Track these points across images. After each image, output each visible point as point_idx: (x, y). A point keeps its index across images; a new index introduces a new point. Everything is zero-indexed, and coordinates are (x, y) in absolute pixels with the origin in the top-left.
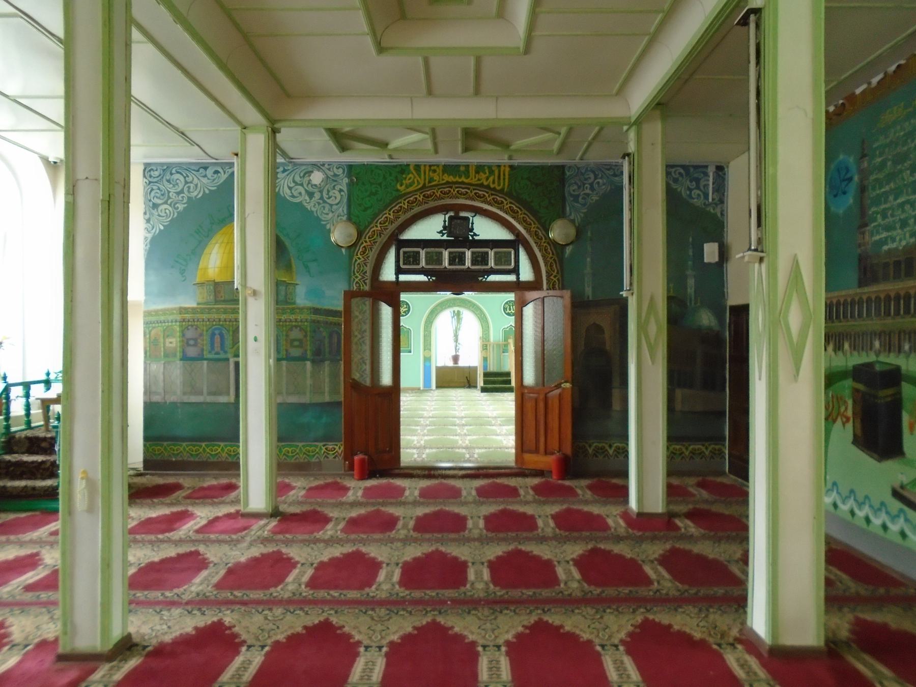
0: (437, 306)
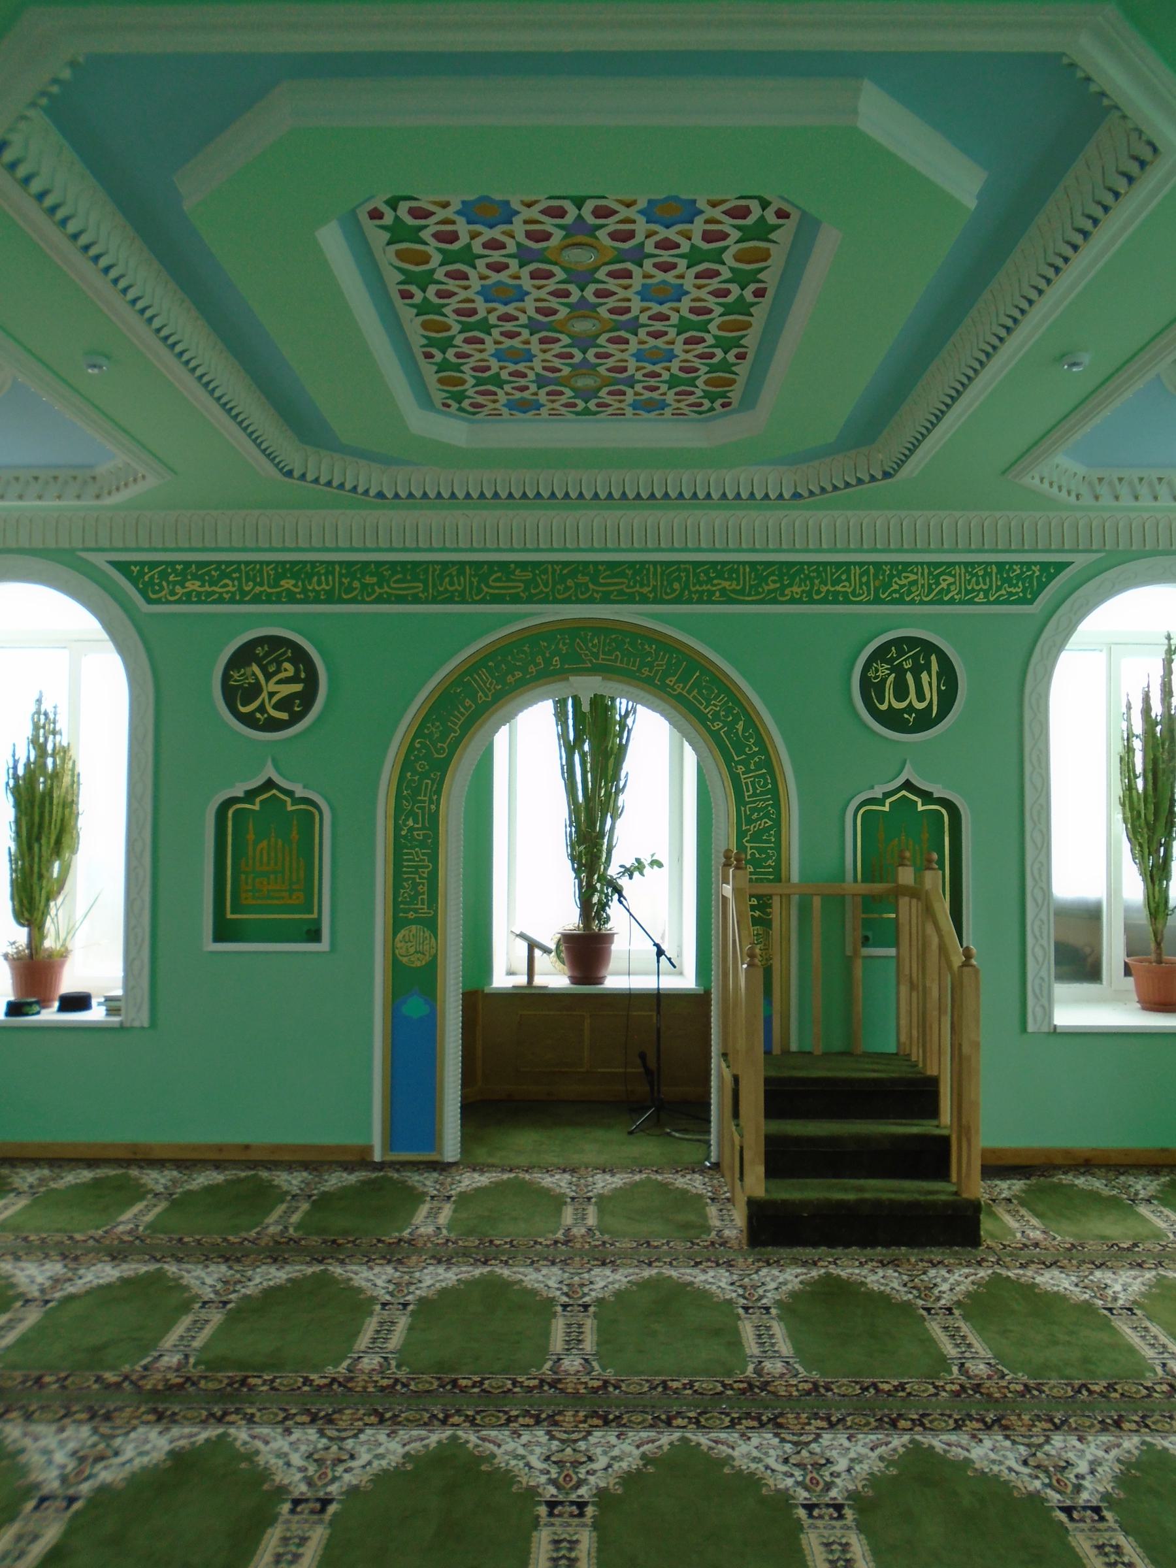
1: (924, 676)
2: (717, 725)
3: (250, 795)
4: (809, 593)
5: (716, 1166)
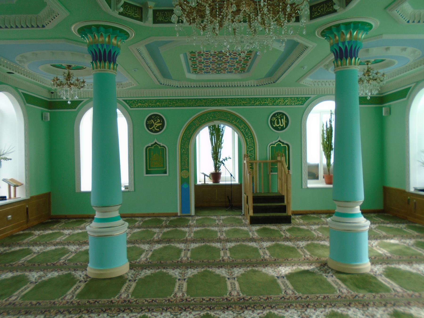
0: (195, 120)
1: (282, 120)
2: (243, 130)
3: (152, 145)
4: (260, 104)
5: (244, 215)
